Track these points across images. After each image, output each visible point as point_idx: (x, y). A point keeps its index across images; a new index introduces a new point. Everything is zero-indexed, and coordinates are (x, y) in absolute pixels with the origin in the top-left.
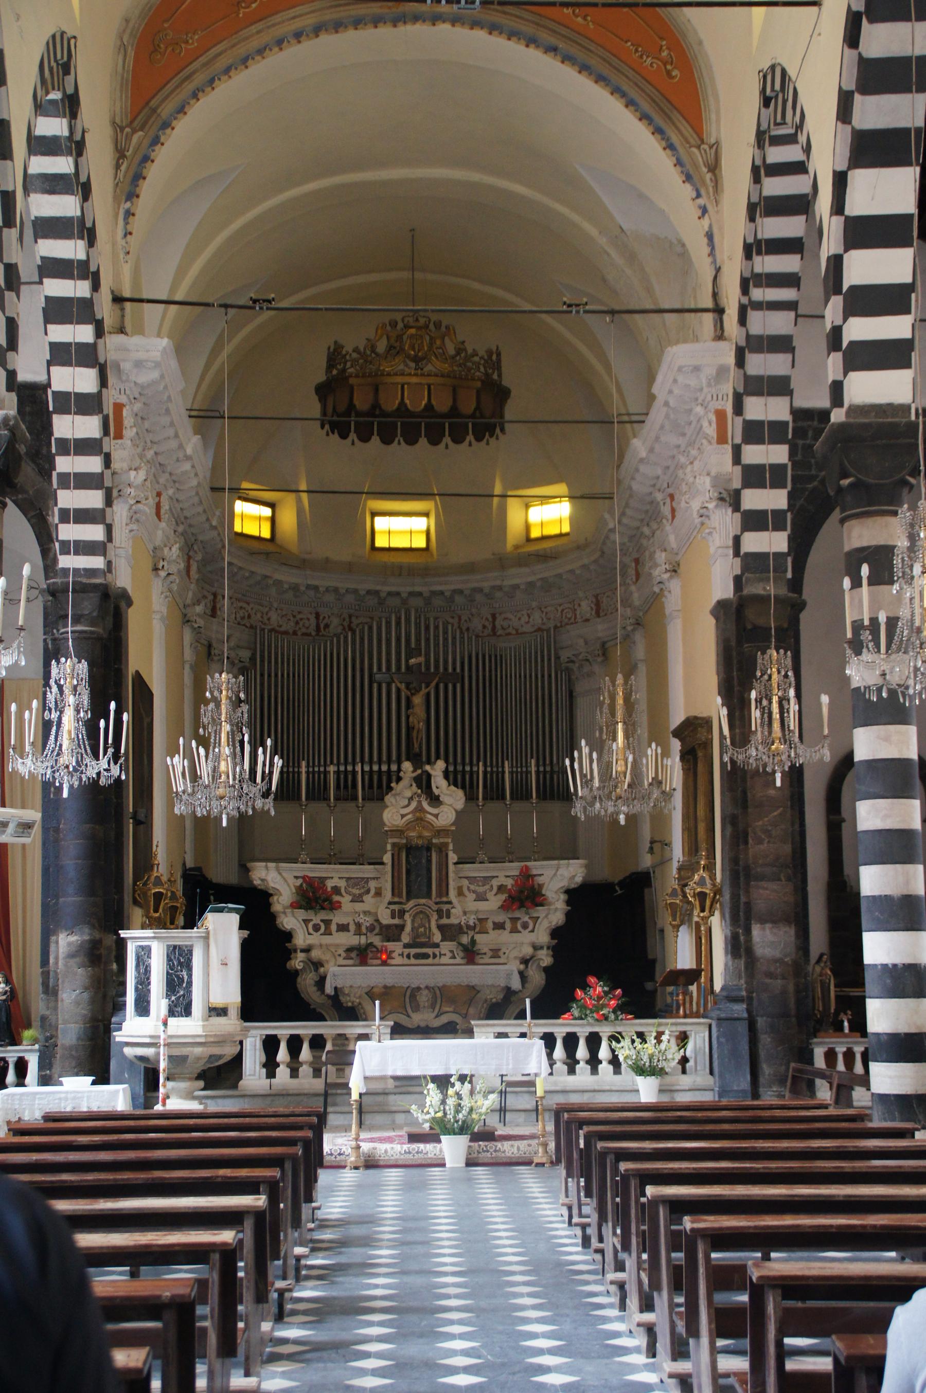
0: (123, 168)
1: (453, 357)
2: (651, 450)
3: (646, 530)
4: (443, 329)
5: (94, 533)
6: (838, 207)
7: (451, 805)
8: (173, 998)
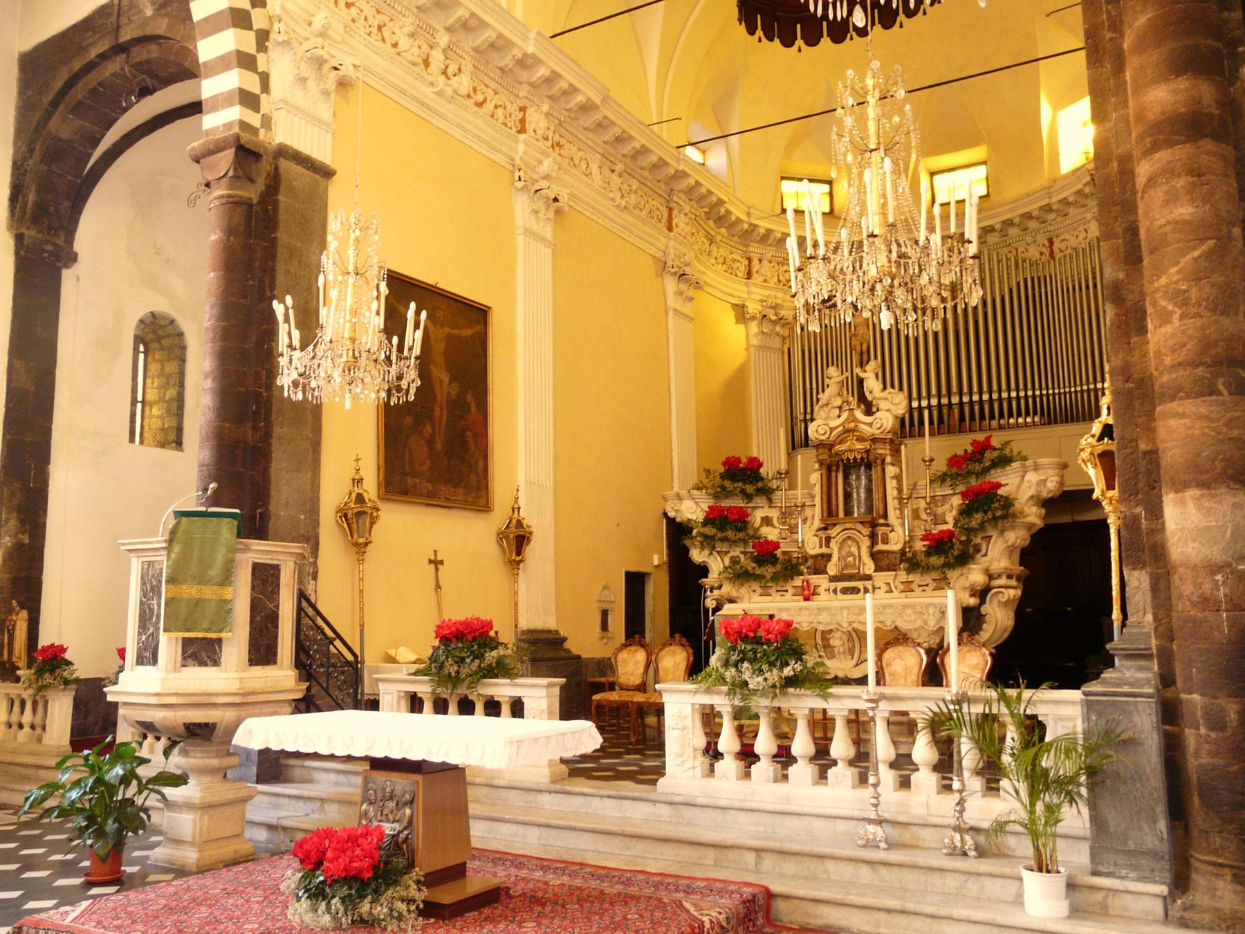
7: (888, 410)
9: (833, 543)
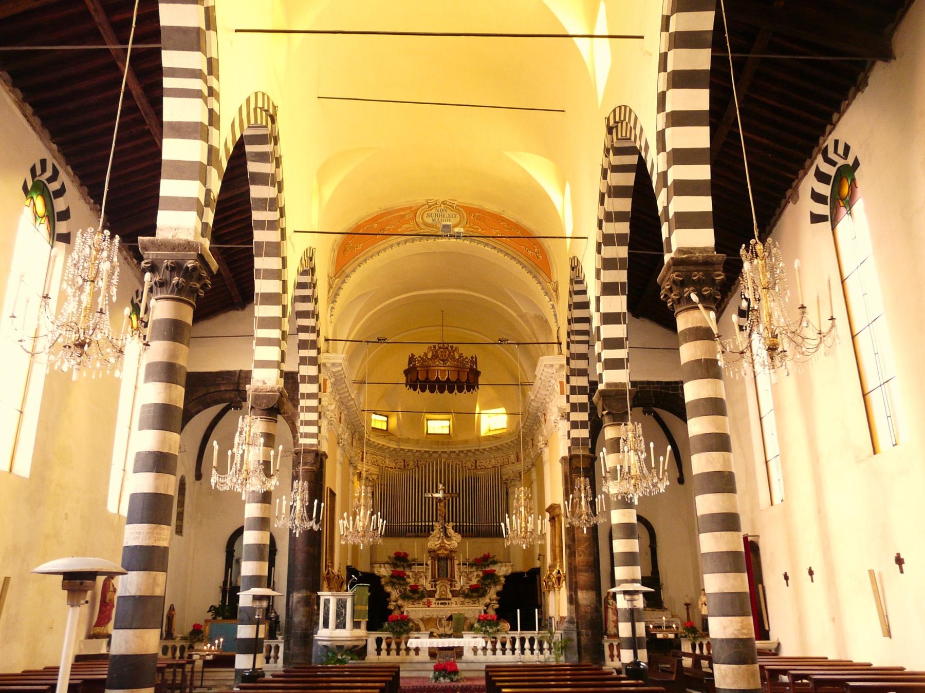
0: (331, 292)
1: (458, 359)
2: (536, 396)
3: (536, 428)
4: (454, 349)
5: (313, 429)
6: (598, 310)
9: (437, 587)
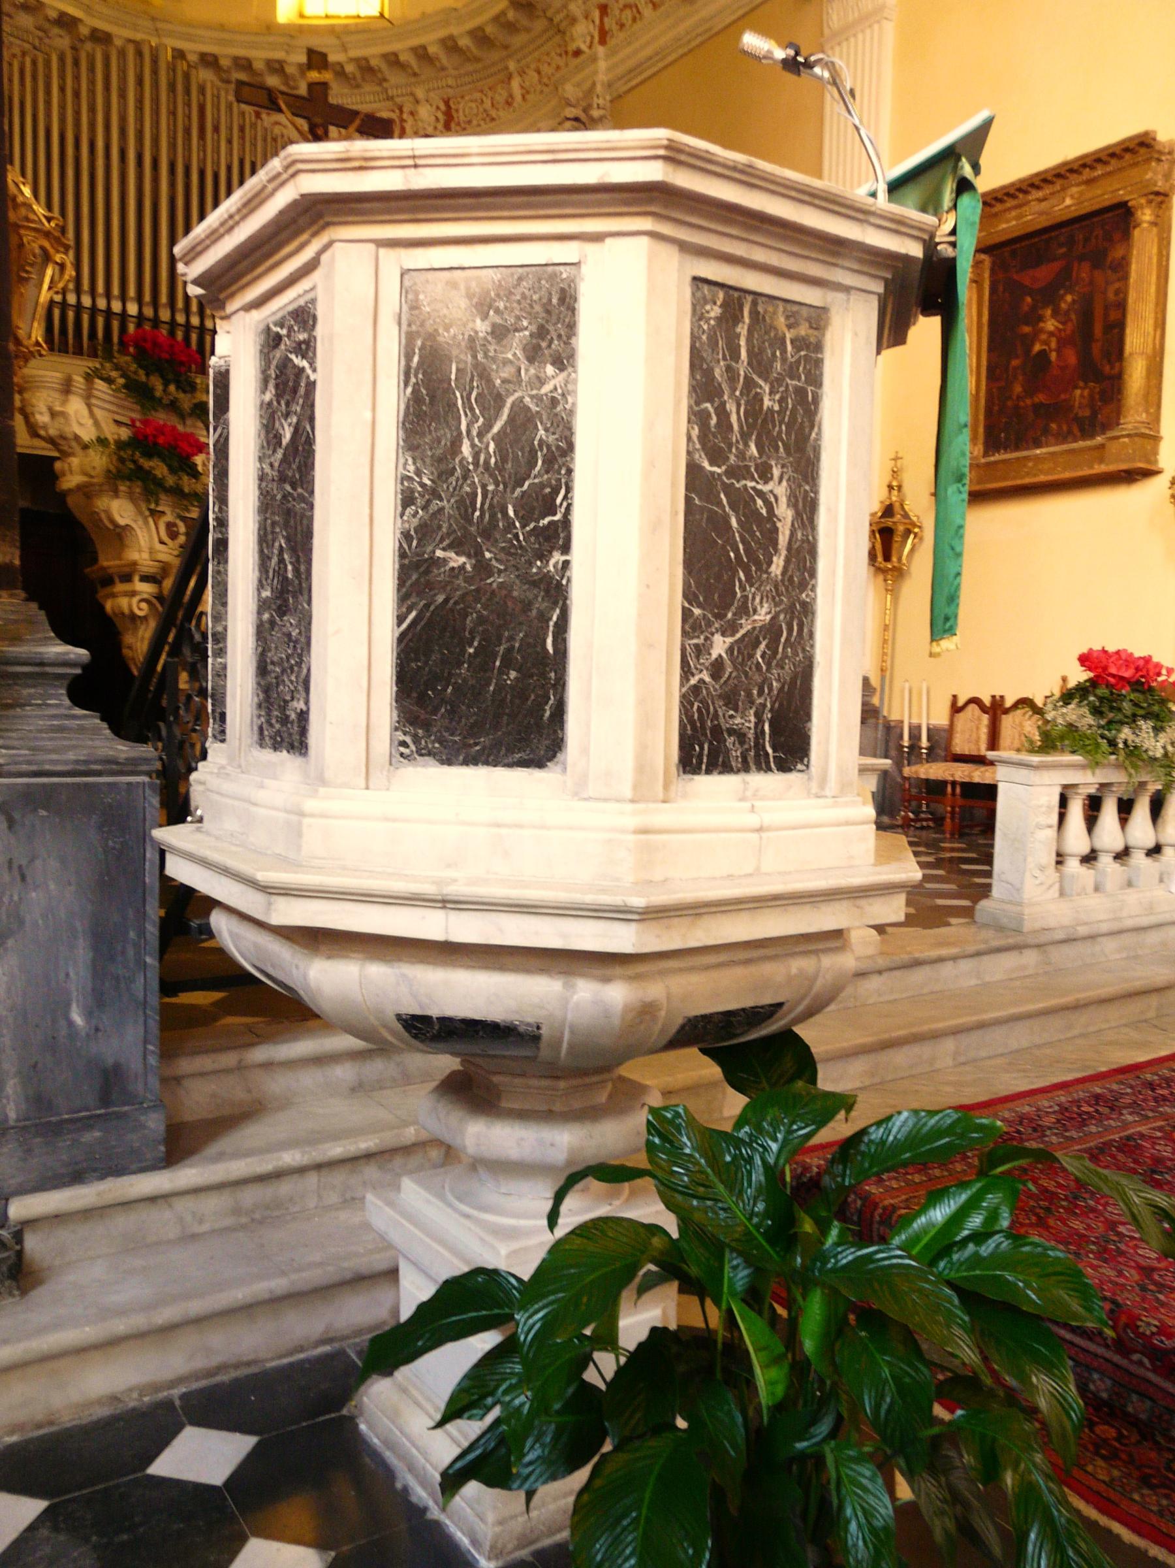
8: (720, 646)
